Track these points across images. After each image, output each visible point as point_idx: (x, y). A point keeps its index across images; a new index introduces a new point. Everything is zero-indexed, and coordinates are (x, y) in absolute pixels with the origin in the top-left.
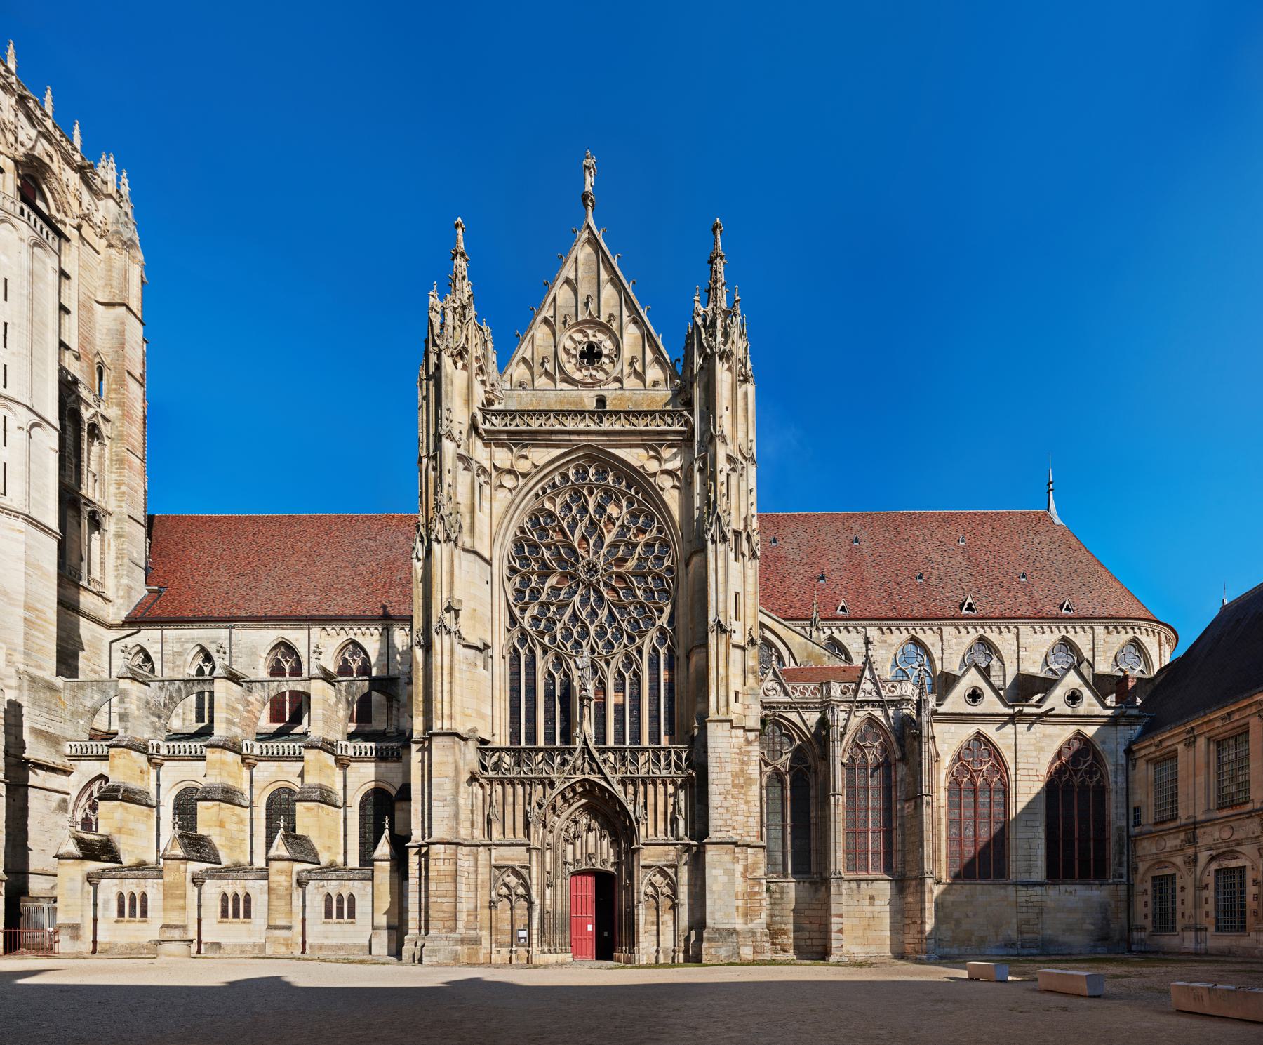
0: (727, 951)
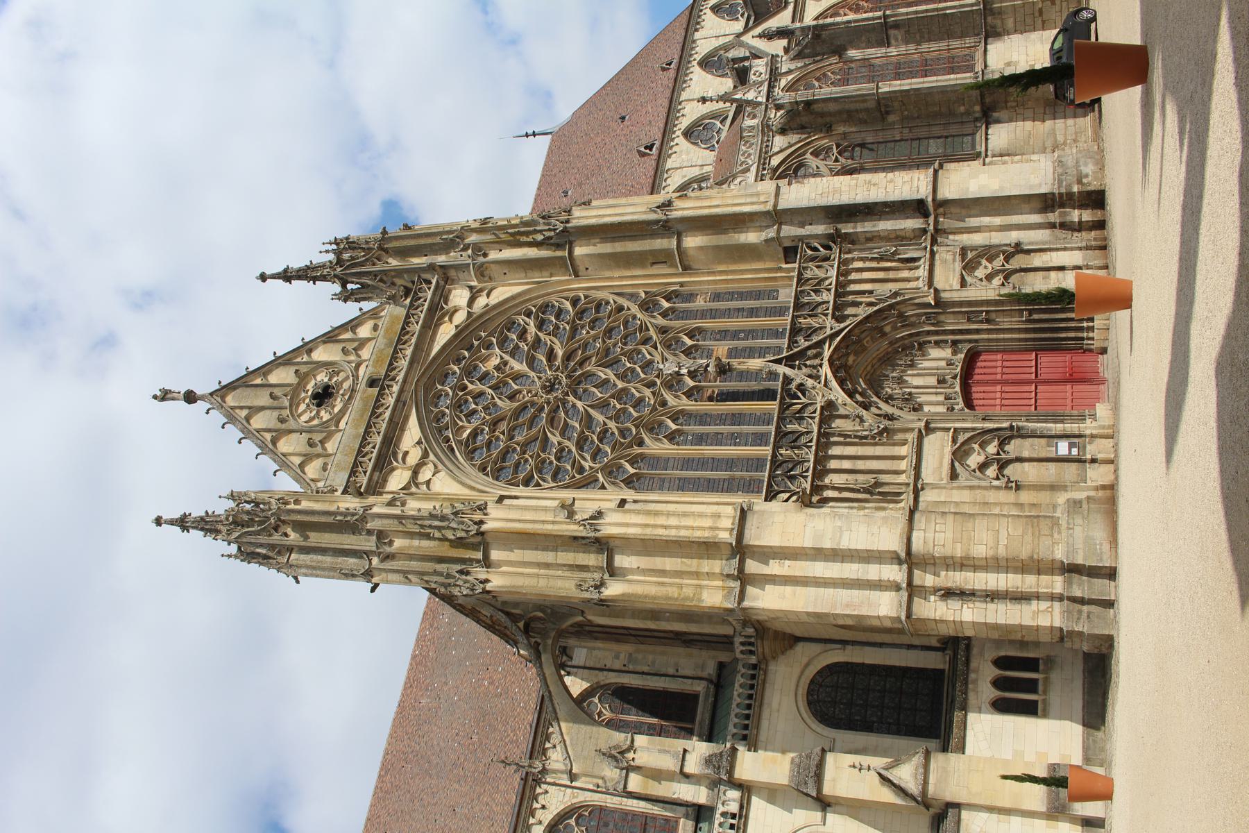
0: (1086, 165)
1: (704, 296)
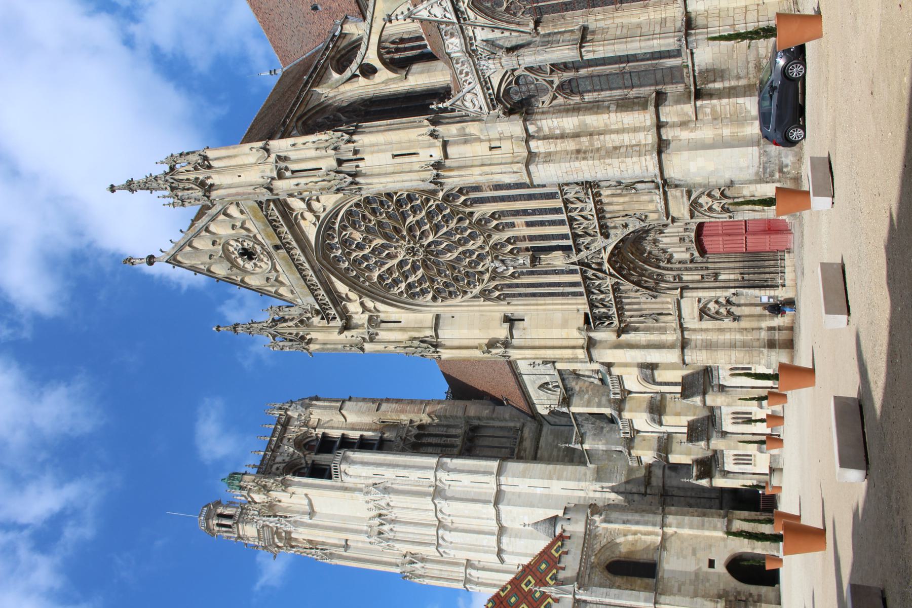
0: (786, 156)
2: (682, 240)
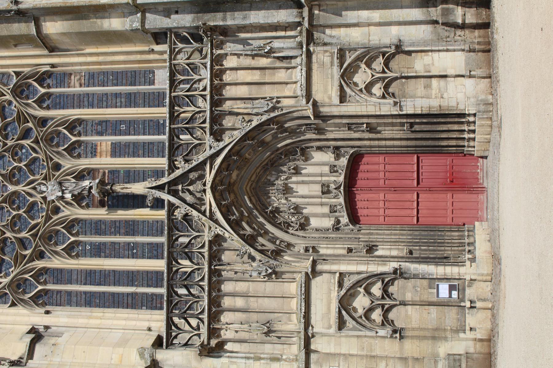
1: (78, 77)
2: (326, 191)
